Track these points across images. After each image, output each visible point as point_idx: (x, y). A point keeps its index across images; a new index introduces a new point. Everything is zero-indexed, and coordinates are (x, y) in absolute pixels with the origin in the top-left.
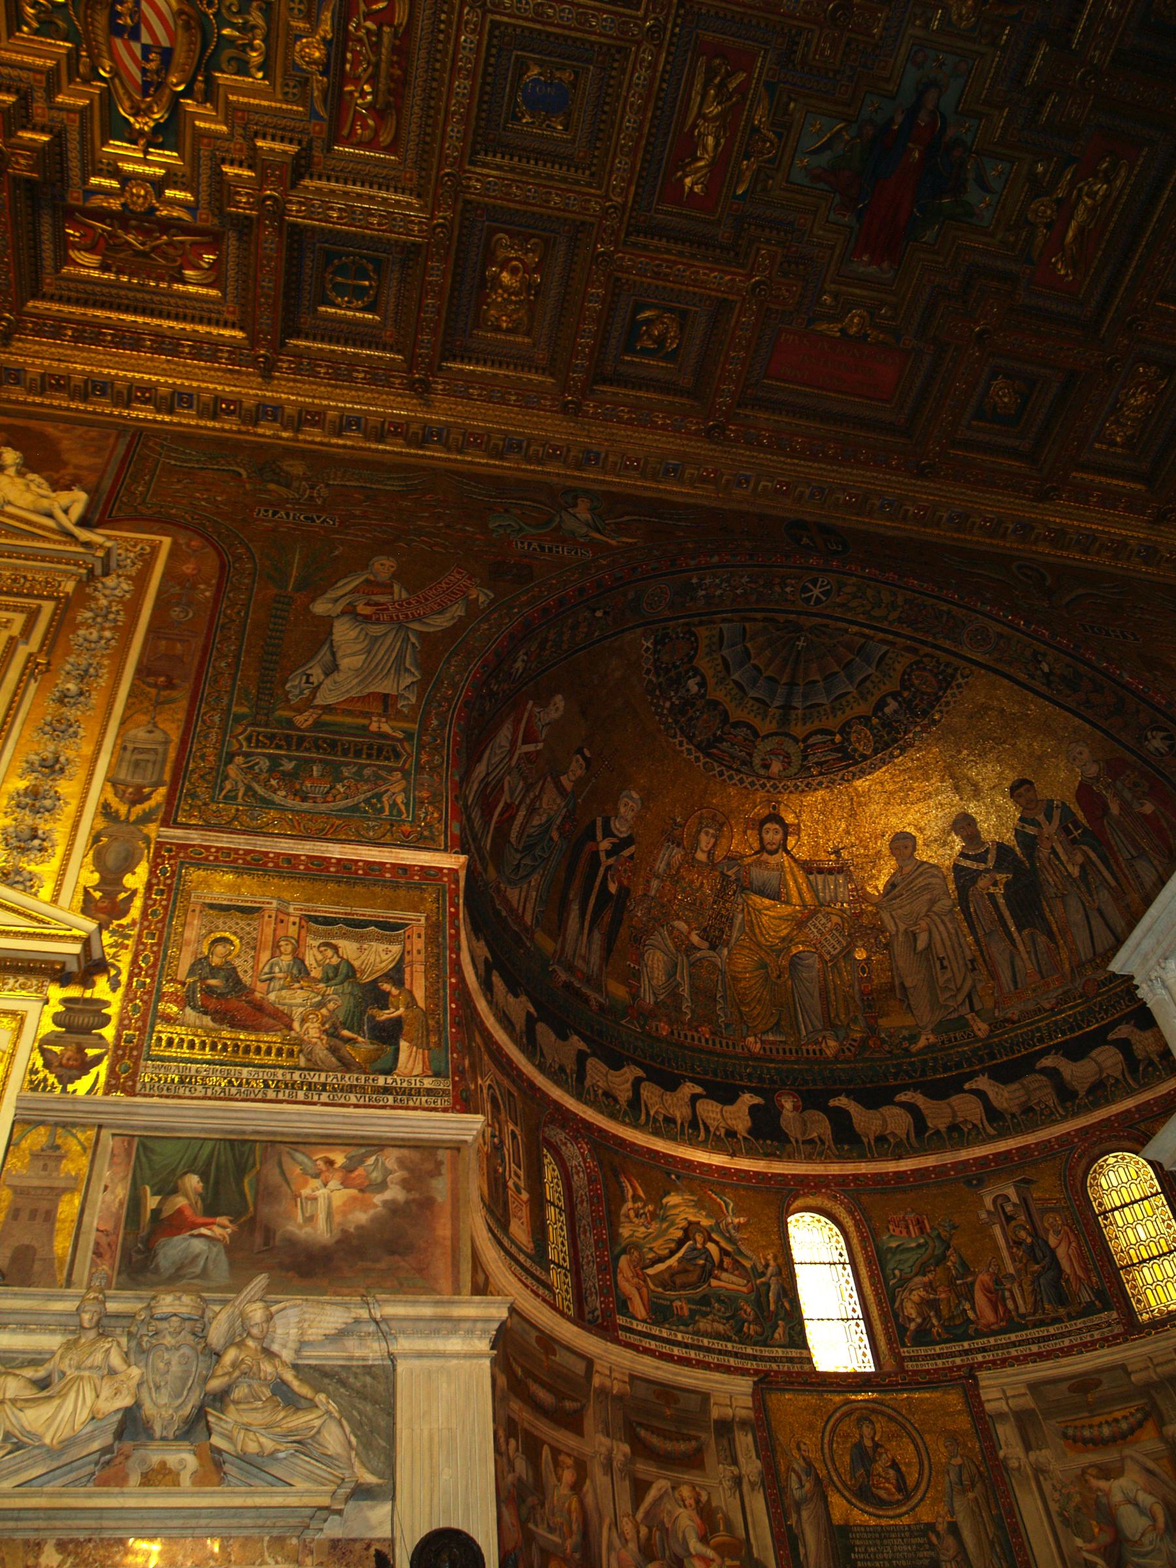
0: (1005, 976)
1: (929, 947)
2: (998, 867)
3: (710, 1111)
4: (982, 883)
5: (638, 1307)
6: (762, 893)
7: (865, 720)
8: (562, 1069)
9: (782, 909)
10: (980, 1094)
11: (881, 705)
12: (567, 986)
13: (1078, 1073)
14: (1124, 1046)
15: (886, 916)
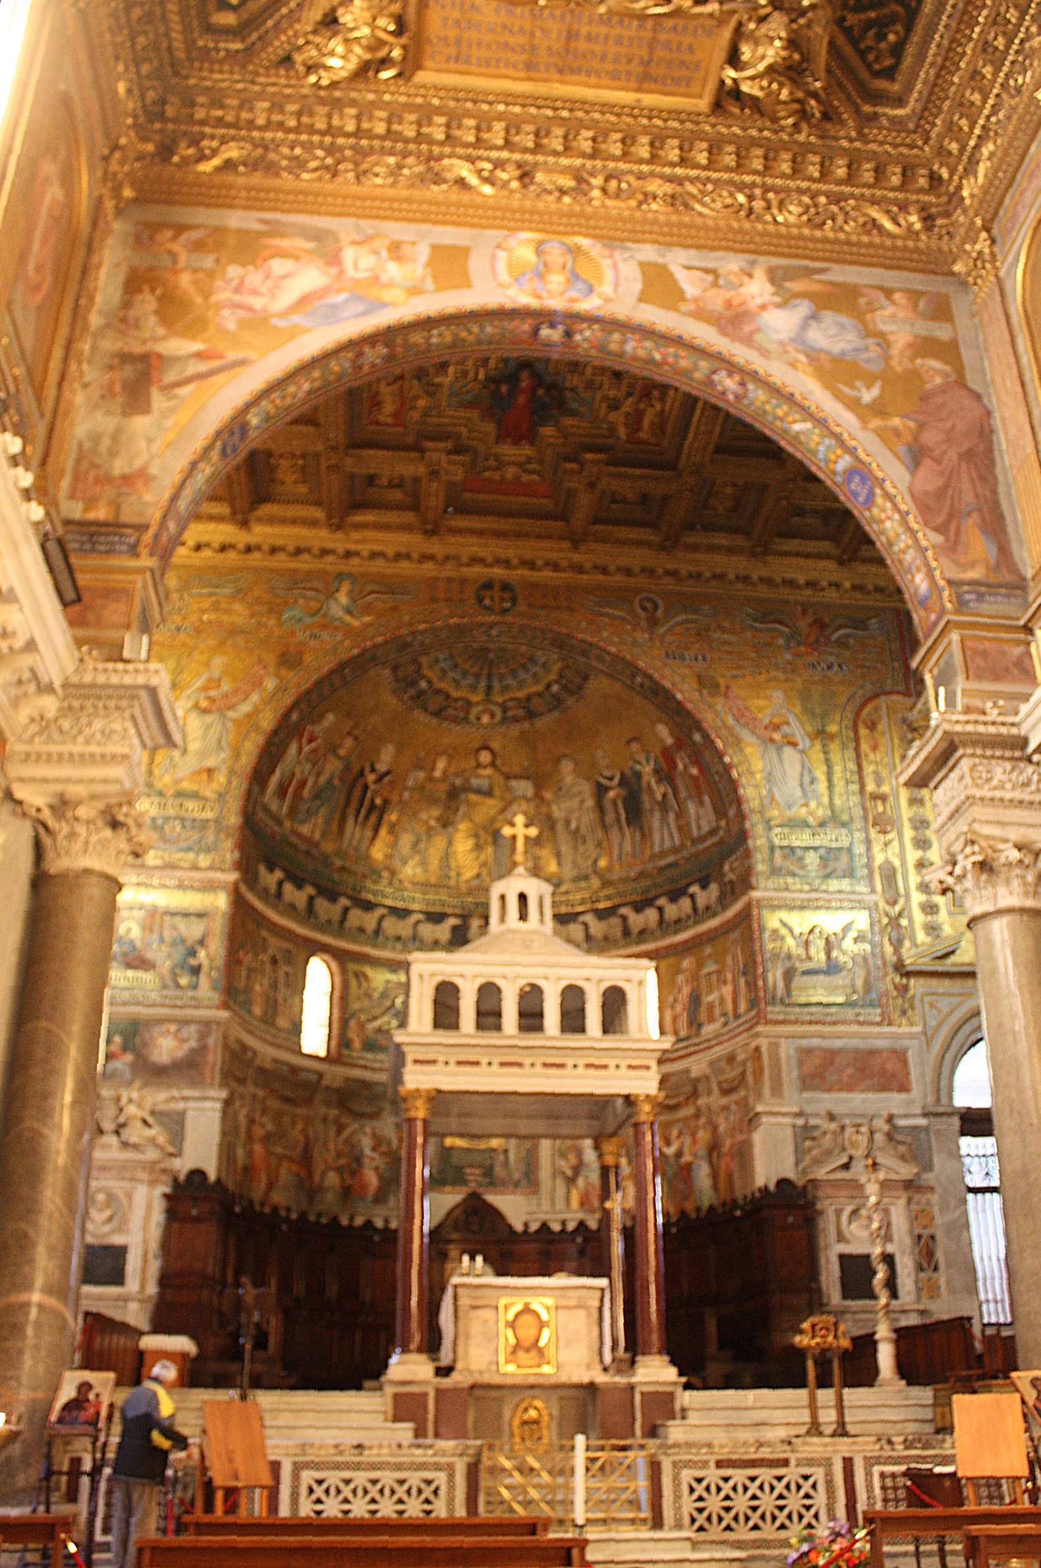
0: (616, 851)
1: (578, 829)
2: (621, 784)
3: (428, 931)
4: (611, 794)
5: (357, 1044)
6: (478, 791)
7: (539, 694)
8: (329, 921)
9: (490, 802)
10: (585, 925)
11: (548, 686)
12: (343, 869)
13: (636, 920)
14: (660, 910)
15: (555, 809)
